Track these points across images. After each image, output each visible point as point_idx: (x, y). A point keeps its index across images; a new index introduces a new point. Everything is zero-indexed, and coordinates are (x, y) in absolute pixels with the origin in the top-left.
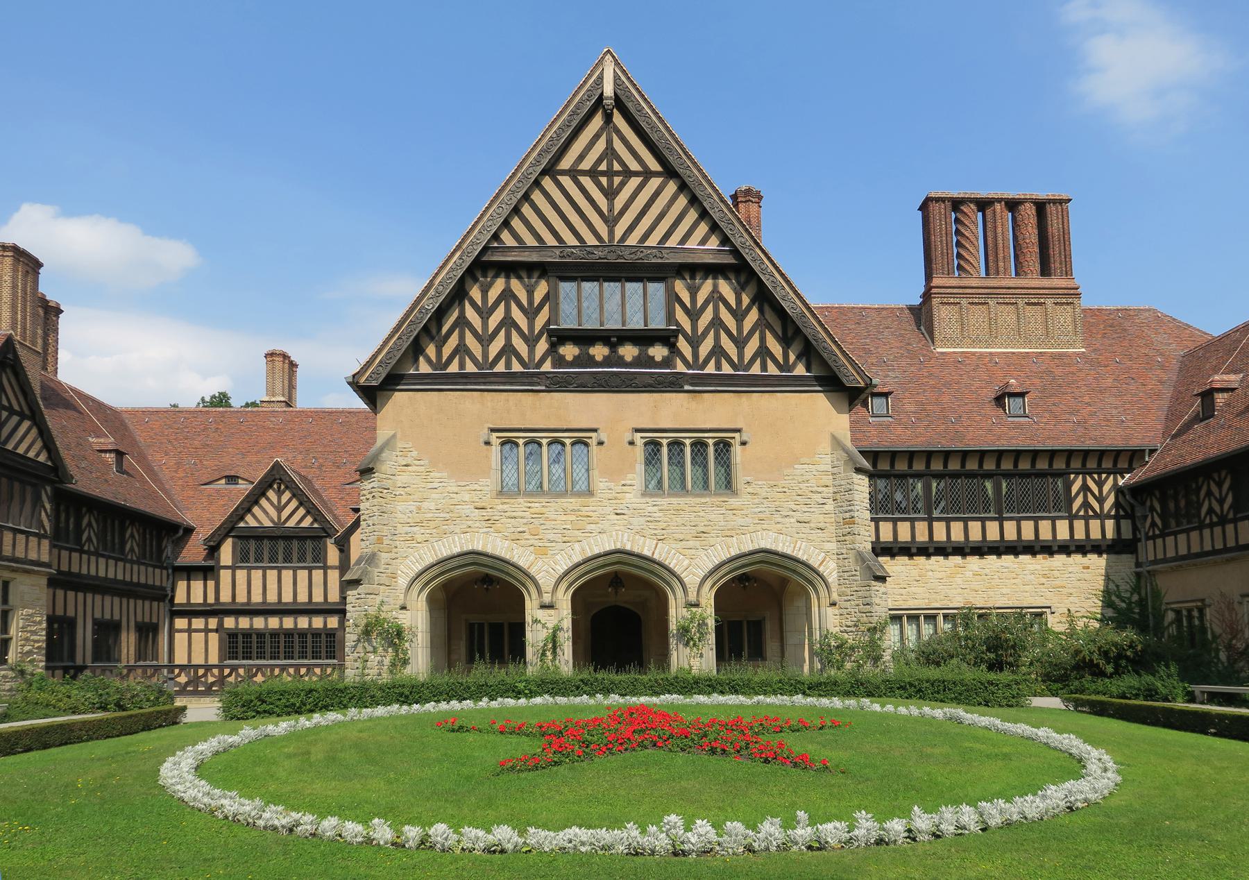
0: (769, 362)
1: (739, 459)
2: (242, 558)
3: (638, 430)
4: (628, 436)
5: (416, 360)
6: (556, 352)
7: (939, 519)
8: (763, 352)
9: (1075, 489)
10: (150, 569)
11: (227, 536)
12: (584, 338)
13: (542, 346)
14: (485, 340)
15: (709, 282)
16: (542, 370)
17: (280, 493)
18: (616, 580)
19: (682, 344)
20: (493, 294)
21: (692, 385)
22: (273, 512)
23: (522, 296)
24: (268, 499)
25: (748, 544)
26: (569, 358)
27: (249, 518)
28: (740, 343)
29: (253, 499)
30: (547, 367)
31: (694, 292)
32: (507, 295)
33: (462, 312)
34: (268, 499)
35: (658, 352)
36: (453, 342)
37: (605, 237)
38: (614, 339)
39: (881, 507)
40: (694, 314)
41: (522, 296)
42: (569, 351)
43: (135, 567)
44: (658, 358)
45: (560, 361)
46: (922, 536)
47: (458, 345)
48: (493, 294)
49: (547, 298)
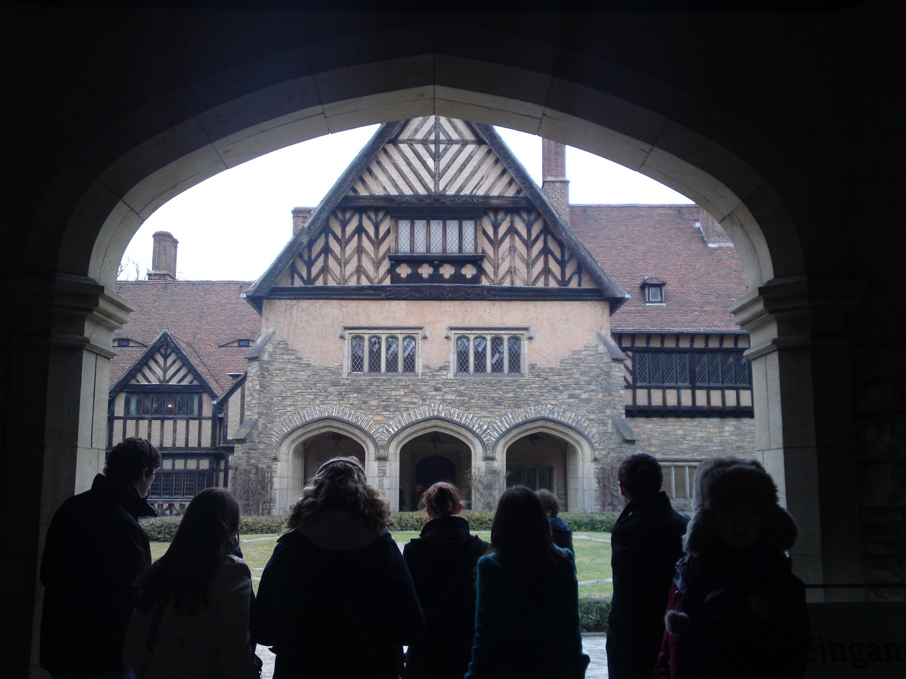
0: (550, 278)
3: (452, 329)
4: (445, 333)
5: (293, 278)
6: (394, 270)
7: (700, 388)
8: (546, 271)
11: (121, 391)
12: (415, 261)
13: (385, 265)
14: (343, 263)
15: (508, 219)
16: (384, 284)
17: (166, 357)
18: (435, 437)
20: (350, 229)
21: (494, 295)
22: (160, 372)
23: (371, 231)
24: (156, 362)
25: (532, 412)
26: (404, 275)
28: (530, 265)
29: (143, 363)
30: (387, 282)
31: (496, 227)
32: (360, 230)
33: (327, 243)
34: (156, 362)
35: (469, 271)
36: (319, 264)
37: (431, 186)
38: (436, 262)
40: (496, 243)
41: (371, 231)
42: (404, 271)
44: (469, 276)
45: (395, 278)
46: (686, 401)
48: (350, 229)
49: (388, 232)
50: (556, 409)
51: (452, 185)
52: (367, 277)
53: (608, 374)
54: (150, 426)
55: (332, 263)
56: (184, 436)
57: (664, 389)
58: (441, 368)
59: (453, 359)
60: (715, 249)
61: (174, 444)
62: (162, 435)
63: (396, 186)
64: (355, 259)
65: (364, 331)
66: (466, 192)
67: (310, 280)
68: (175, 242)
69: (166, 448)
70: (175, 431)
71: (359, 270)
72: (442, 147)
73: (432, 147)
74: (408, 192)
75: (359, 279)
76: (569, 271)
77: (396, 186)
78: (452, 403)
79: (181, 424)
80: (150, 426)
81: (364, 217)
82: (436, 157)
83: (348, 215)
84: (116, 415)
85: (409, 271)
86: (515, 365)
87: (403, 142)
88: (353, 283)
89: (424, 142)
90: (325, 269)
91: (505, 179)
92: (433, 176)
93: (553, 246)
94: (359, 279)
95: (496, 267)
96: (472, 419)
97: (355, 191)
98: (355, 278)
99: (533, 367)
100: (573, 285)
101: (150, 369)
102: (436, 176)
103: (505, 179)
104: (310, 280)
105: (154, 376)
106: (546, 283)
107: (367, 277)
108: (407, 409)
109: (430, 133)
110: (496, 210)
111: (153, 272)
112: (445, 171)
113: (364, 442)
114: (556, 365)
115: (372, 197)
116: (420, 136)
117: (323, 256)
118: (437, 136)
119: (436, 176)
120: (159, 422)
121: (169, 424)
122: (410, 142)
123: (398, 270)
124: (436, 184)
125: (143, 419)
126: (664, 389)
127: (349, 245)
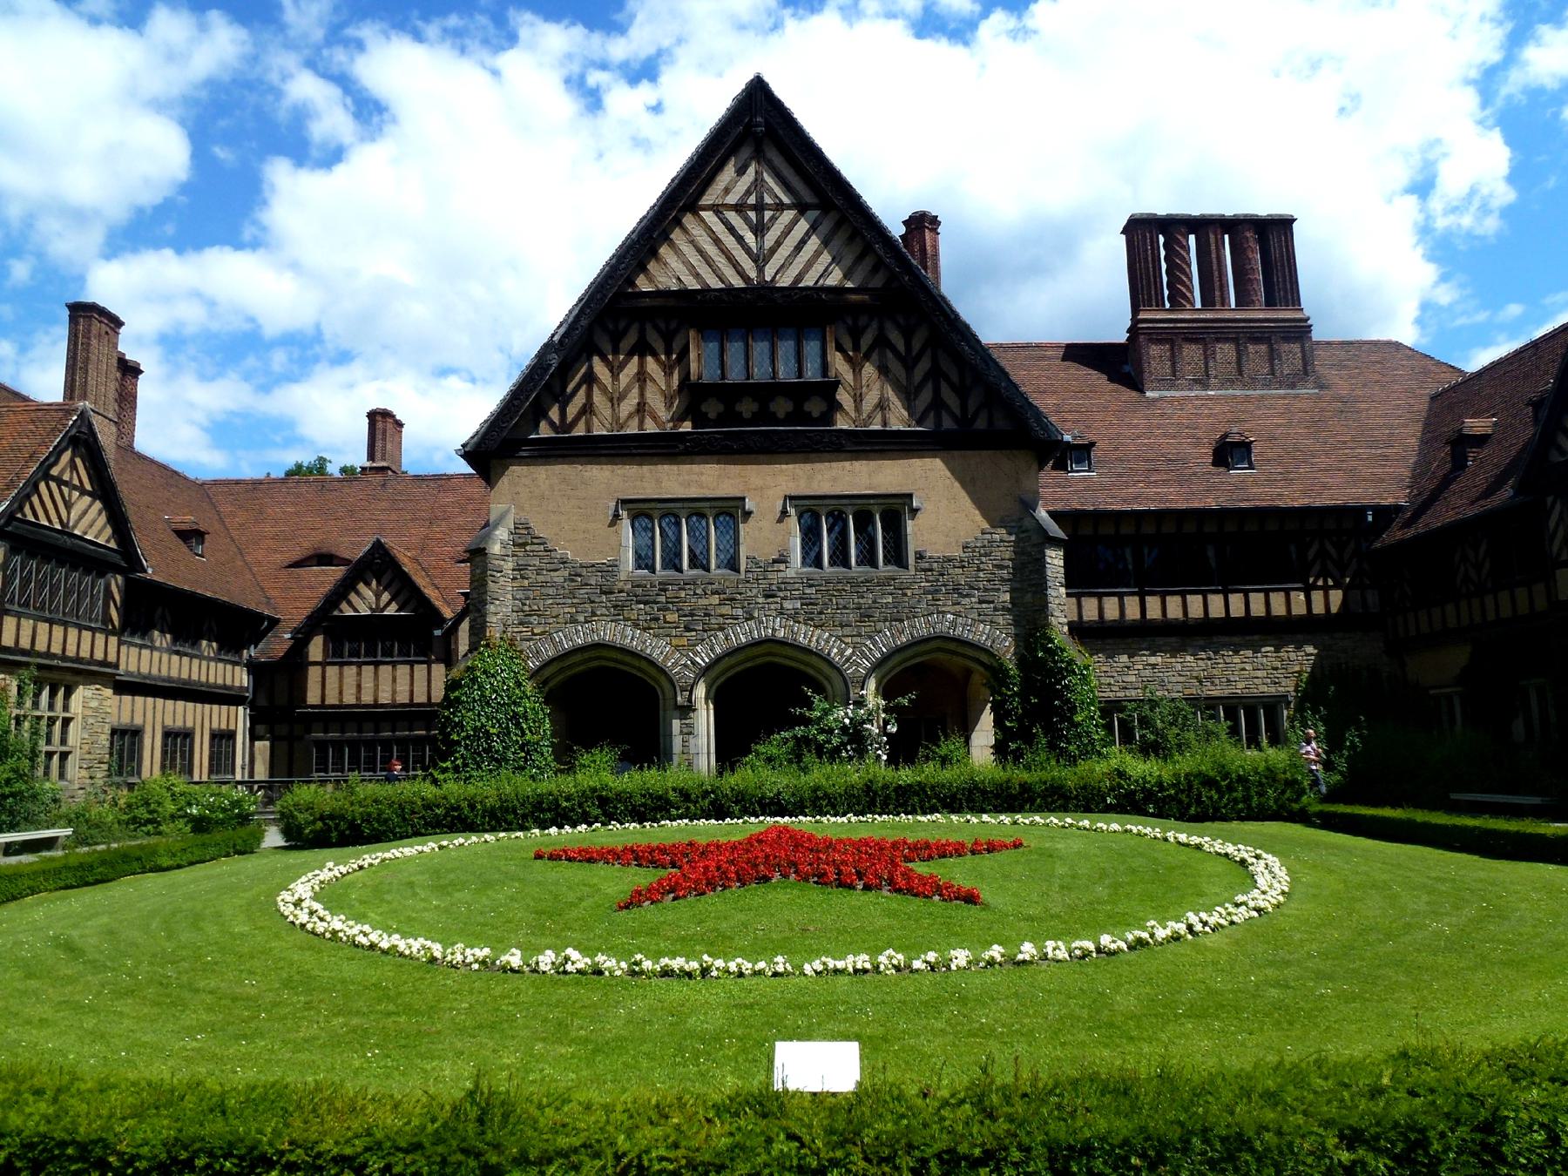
1: (909, 530)
2: (335, 656)
7: (1152, 594)
9: (1311, 554)
10: (229, 667)
12: (728, 393)
14: (615, 400)
15: (875, 325)
19: (843, 396)
25: (922, 628)
27: (344, 606)
33: (591, 368)
36: (579, 400)
37: (753, 274)
39: (1077, 581)
43: (212, 664)
44: (816, 414)
47: (585, 405)
50: (960, 620)
51: (783, 272)
52: (655, 418)
53: (1041, 564)
54: (359, 674)
55: (598, 398)
56: (407, 688)
57: (1100, 596)
58: (775, 561)
59: (796, 542)
60: (1155, 400)
61: (394, 699)
62: (376, 686)
63: (697, 276)
64: (635, 391)
65: (653, 505)
66: (809, 281)
67: (566, 426)
68: (400, 425)
69: (383, 706)
70: (394, 680)
71: (641, 409)
72: (768, 214)
73: (752, 215)
74: (715, 284)
75: (641, 422)
76: (972, 405)
77: (697, 276)
78: (794, 616)
79: (403, 670)
80: (359, 674)
81: (648, 327)
82: (759, 230)
83: (622, 325)
84: (312, 659)
85: (721, 408)
86: (897, 554)
87: (706, 208)
88: (632, 429)
89: (739, 208)
90: (588, 409)
91: (868, 262)
92: (755, 261)
93: (946, 365)
94: (641, 422)
95: (858, 399)
96: (827, 641)
97: (633, 284)
98: (635, 422)
99: (920, 556)
100: (981, 424)
101: (358, 593)
102: (760, 260)
103: (868, 262)
104: (566, 426)
105: (365, 601)
106: (938, 422)
107: (655, 418)
108: (722, 629)
109: (748, 193)
110: (858, 309)
111: (368, 464)
112: (773, 251)
113: (657, 681)
114: (957, 553)
115: (659, 294)
116: (732, 199)
117: (584, 387)
118: (760, 198)
119: (760, 260)
120: (371, 668)
121: (385, 670)
122: (717, 209)
123: (704, 408)
124: (761, 270)
125: (351, 663)
126: (1100, 596)
127: (626, 371)
